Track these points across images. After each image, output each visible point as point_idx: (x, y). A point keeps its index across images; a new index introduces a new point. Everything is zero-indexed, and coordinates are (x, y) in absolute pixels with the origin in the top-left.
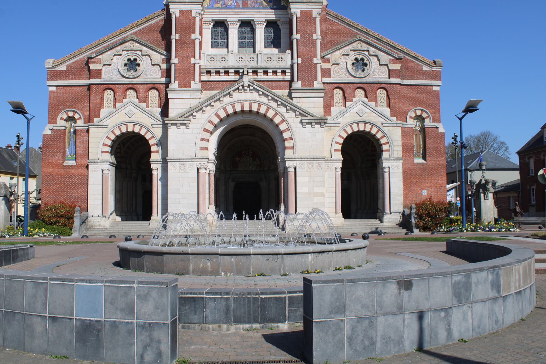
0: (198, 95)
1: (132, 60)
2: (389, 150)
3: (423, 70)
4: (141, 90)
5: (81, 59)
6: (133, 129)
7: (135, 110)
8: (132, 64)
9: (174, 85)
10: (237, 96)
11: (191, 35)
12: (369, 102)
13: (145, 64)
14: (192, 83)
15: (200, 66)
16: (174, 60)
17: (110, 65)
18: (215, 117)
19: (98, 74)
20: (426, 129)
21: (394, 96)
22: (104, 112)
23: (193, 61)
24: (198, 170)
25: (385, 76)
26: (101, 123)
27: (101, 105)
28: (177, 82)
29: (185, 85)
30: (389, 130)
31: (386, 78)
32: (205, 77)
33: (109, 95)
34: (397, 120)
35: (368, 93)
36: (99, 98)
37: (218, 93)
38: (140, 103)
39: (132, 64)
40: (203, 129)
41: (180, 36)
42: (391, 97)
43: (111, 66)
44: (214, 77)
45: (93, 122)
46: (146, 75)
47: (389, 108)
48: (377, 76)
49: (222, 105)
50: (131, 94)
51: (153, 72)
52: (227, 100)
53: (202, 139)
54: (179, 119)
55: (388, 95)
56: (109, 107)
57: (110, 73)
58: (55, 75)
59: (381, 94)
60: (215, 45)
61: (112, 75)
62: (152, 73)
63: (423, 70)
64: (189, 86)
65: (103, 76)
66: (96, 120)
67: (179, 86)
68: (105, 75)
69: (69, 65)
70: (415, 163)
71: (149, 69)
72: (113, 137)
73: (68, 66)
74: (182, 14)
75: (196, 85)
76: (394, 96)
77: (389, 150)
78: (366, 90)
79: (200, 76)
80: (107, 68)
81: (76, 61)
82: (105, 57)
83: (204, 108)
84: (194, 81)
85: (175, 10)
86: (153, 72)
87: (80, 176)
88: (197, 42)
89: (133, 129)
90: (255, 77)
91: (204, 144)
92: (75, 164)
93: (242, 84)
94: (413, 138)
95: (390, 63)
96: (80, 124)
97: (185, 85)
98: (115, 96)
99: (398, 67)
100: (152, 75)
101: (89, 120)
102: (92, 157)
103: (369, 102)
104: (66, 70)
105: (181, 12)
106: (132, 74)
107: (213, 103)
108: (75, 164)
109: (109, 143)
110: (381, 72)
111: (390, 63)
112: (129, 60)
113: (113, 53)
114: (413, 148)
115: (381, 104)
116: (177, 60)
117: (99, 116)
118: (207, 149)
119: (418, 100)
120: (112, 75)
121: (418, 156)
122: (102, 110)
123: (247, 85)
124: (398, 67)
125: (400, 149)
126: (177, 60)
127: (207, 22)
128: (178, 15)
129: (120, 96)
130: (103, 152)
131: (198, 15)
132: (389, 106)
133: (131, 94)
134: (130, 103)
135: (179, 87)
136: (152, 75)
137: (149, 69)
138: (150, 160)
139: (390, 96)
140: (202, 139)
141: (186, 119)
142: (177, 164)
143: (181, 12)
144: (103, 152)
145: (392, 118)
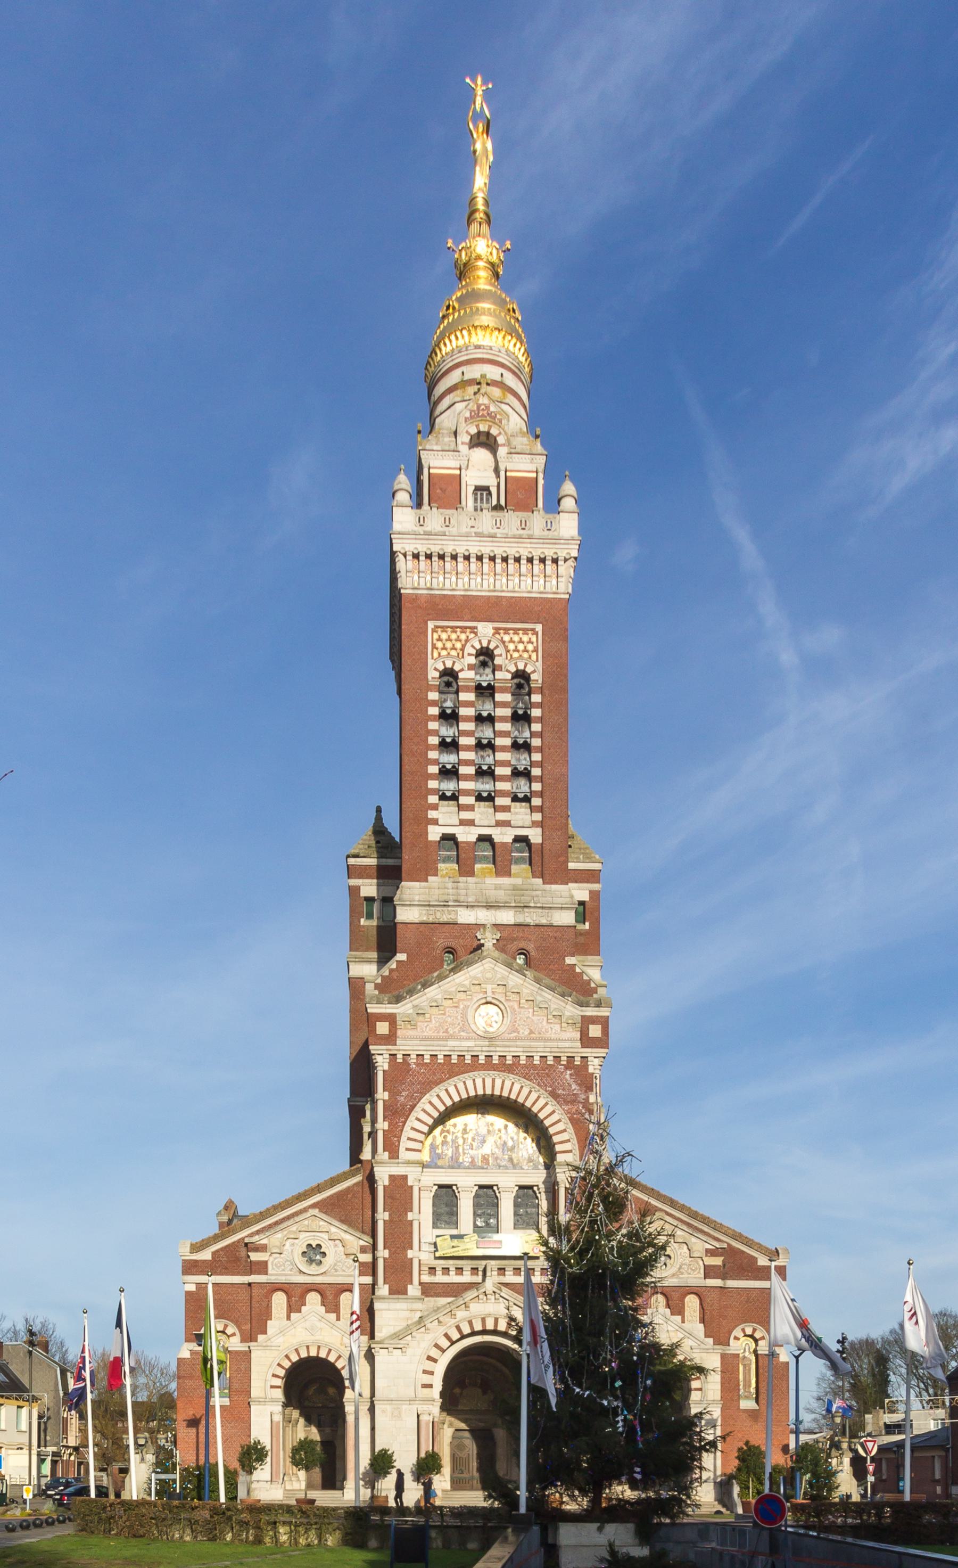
0: (418, 1305)
1: (314, 1246)
2: (700, 1389)
3: (759, 1264)
4: (328, 1293)
5: (234, 1243)
6: (318, 1353)
7: (319, 1325)
8: (314, 1253)
9: (383, 1290)
10: (478, 1309)
11: (406, 1214)
12: (672, 1315)
13: (333, 1253)
14: (410, 1287)
15: (420, 1260)
16: (383, 1253)
17: (281, 1254)
18: (444, 1339)
19: (262, 1268)
20: (759, 1356)
21: (711, 1306)
22: (272, 1326)
23: (410, 1254)
24: (418, 1416)
25: (697, 1276)
26: (269, 1343)
27: (267, 1314)
28: (387, 1286)
29: (398, 1290)
30: (701, 1358)
31: (700, 1278)
32: (426, 1278)
33: (279, 1301)
34: (714, 1344)
35: (670, 1302)
36: (264, 1305)
37: (449, 1303)
38: (327, 1314)
39: (314, 1253)
40: (426, 1357)
41: (390, 1215)
42: (705, 1308)
43: (282, 1256)
44: (440, 1278)
45: (256, 1341)
46: (336, 1270)
47: (702, 1325)
48: (686, 1275)
49: (453, 1321)
50: (313, 1298)
51: (347, 1267)
52: (461, 1314)
53: (425, 1372)
54: (391, 1342)
55: (701, 1304)
56: (279, 1318)
57: (281, 1266)
58: (190, 1268)
59: (692, 1303)
60: (437, 1220)
61: (283, 1270)
62: (344, 1268)
63: (759, 1264)
64: (405, 1293)
65: (270, 1271)
66: (261, 1337)
67: (391, 1292)
68: (273, 1269)
69: (217, 1251)
70: (741, 1408)
71: (340, 1262)
72: (287, 1364)
73: (214, 1254)
74: (394, 1181)
75: (414, 1290)
76: (711, 1306)
77: (700, 1389)
78: (669, 1296)
79: (420, 1274)
80: (275, 1259)
81: (227, 1246)
82: (273, 1240)
83: (429, 1325)
84: (412, 1284)
85: (382, 1175)
86: (347, 1267)
87: (237, 1421)
88: (416, 1225)
89: (318, 1353)
90: (501, 1277)
91: (427, 1379)
92: (228, 1404)
93: (483, 1290)
94: (739, 1369)
95: (706, 1256)
96: (235, 1344)
97: (398, 1290)
98: (288, 1301)
99: (718, 1261)
100: (344, 1271)
101: (249, 1337)
102: (254, 1393)
103: (672, 1315)
104: (210, 1258)
105: (392, 1178)
106: (313, 1269)
107: (441, 1319)
108: (228, 1404)
109: (282, 1373)
110: (692, 1269)
111: (706, 1256)
112: (309, 1245)
113: (286, 1236)
114: (739, 1385)
115: (690, 1318)
116: (387, 1252)
117: (265, 1332)
118: (430, 1386)
119: (748, 1311)
120: (283, 1270)
121: (747, 1398)
122: (269, 1322)
123: (491, 1292)
124: (718, 1261)
125: (719, 1387)
126: (387, 1252)
127: (428, 1189)
128: (387, 1183)
129: (296, 1302)
130: (272, 1387)
131: (416, 1183)
132: (702, 1320)
133: (313, 1298)
134: (313, 1313)
135: (390, 1294)
136: (344, 1271)
137: (340, 1262)
138: (344, 1400)
139: (704, 1305)
140: (425, 1372)
141: (401, 1342)
142: (389, 1408)
143: (392, 1178)
144: (272, 1387)
145: (707, 1339)
